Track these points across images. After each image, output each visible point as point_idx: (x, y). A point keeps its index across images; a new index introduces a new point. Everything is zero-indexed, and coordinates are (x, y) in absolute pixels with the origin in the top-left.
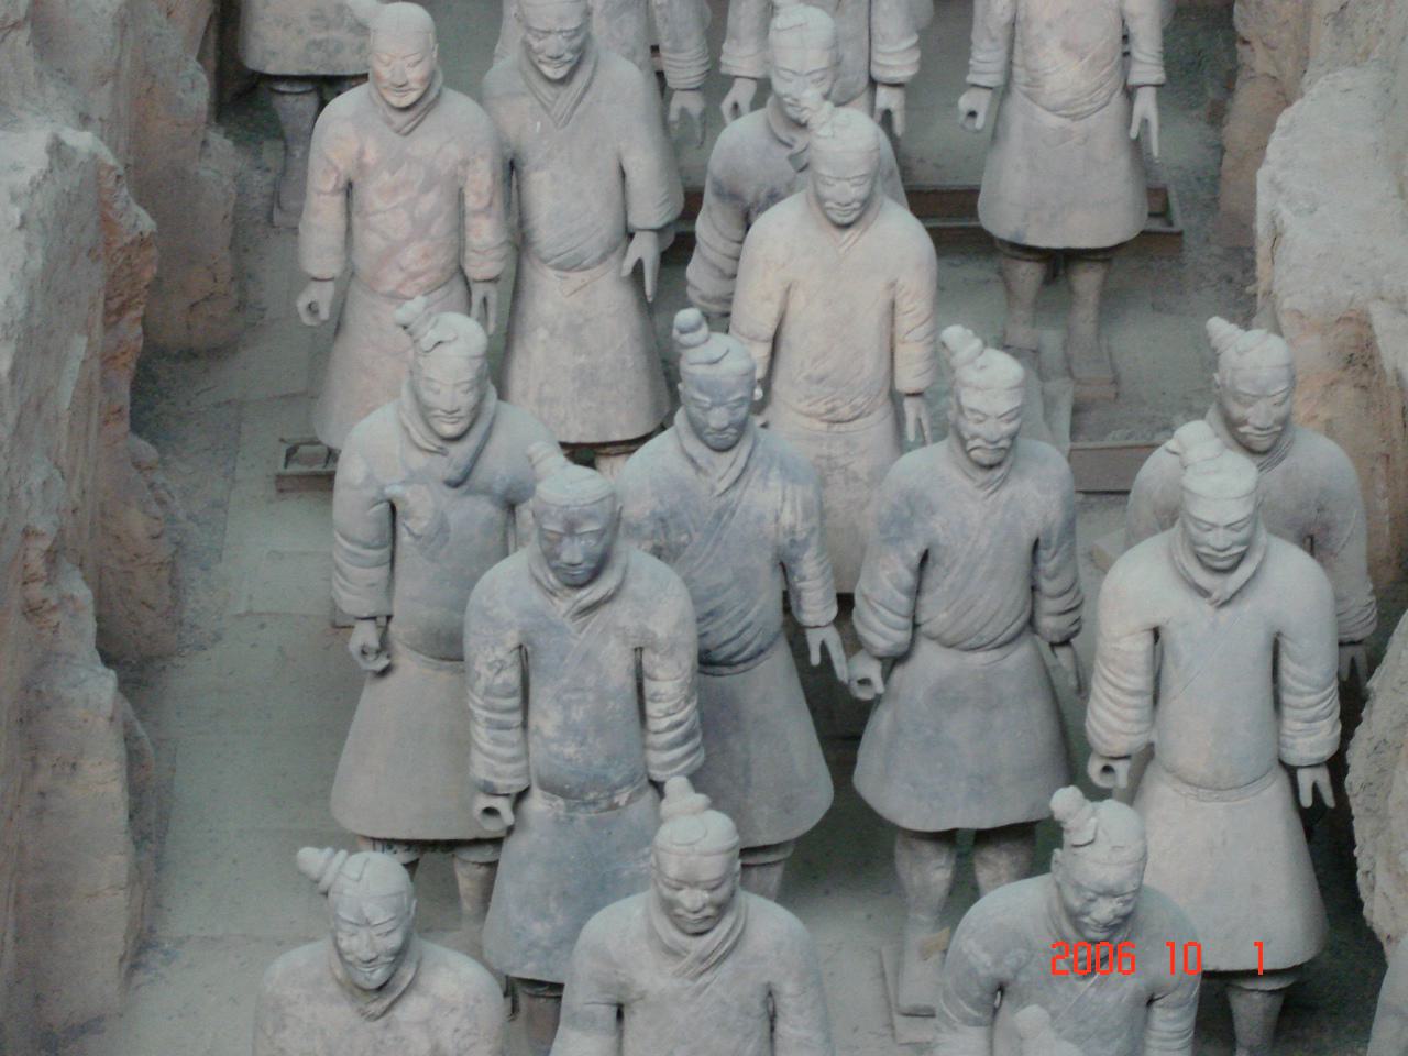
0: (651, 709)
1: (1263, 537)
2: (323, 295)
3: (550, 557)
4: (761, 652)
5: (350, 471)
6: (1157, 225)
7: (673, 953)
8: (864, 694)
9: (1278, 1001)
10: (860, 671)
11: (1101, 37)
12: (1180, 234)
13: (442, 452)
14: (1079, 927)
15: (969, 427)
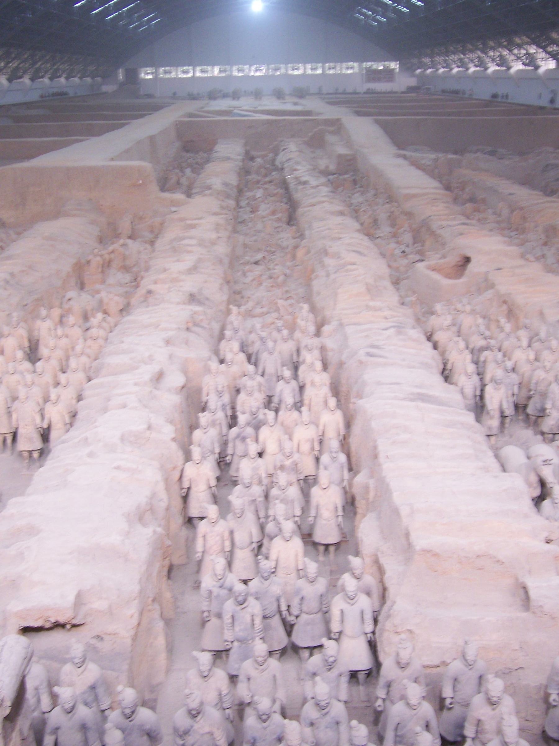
0: (255, 626)
1: (359, 594)
2: (199, 555)
3: (236, 599)
4: (274, 616)
5: (203, 585)
6: (344, 539)
7: (257, 669)
8: (293, 623)
9: (366, 675)
10: (291, 619)
11: (331, 507)
12: (348, 540)
13: (219, 582)
14: (328, 663)
15: (309, 575)
